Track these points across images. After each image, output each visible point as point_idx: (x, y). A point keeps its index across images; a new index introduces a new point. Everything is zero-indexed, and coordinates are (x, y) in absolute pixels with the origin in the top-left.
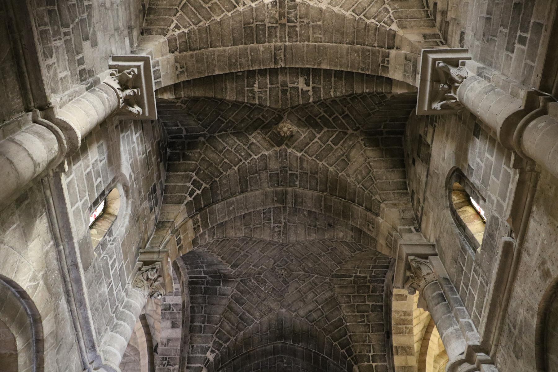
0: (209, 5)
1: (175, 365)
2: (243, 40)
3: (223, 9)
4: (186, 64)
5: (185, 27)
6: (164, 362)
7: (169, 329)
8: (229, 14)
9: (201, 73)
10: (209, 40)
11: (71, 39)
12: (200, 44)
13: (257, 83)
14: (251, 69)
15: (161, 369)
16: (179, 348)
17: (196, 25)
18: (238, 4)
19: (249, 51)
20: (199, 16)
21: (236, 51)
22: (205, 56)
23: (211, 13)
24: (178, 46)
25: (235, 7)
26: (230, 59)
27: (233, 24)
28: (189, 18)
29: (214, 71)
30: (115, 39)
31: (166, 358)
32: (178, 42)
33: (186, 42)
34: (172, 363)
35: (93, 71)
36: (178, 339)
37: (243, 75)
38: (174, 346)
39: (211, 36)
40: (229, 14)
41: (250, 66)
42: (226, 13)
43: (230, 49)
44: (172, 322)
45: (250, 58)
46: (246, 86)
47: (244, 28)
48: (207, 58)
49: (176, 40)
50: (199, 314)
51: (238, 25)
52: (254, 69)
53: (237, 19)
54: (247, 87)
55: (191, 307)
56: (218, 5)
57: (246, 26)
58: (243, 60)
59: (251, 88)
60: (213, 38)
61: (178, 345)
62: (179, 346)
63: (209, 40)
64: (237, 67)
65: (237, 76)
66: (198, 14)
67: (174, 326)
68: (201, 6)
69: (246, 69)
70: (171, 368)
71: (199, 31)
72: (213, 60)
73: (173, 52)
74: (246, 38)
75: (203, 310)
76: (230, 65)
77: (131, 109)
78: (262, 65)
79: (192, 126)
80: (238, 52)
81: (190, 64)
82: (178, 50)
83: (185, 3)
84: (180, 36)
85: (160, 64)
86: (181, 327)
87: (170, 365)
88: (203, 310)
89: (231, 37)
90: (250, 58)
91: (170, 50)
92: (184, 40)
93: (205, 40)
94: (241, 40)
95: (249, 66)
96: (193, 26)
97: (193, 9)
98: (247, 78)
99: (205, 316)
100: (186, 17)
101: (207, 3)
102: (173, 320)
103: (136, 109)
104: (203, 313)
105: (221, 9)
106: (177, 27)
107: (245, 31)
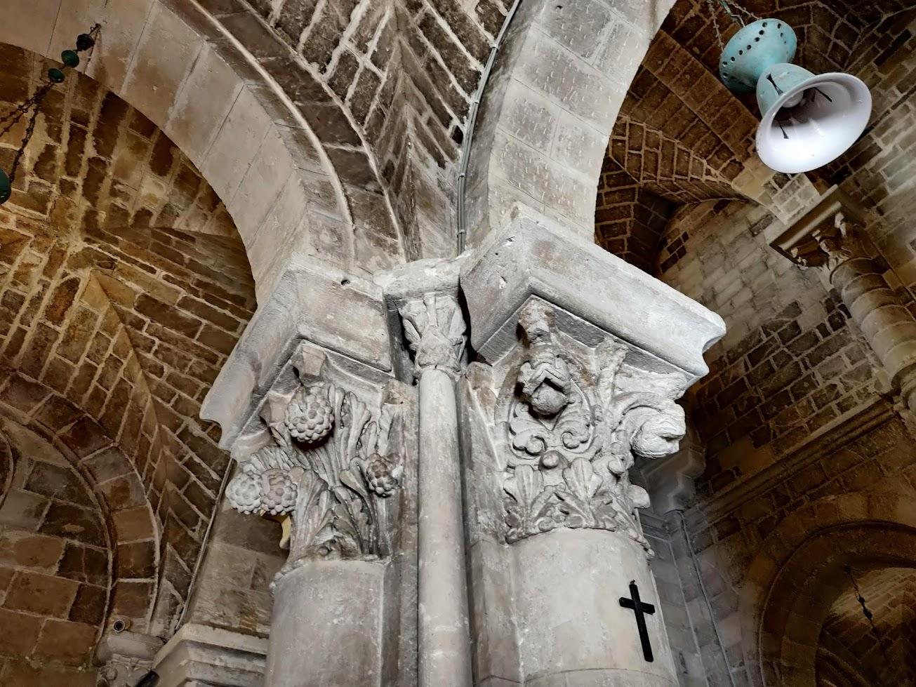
0: (655, 150)
2: (655, 85)
3: (645, 134)
4: (741, 139)
5: (702, 164)
8: (644, 125)
9: (737, 110)
10: (691, 125)
11: (807, 356)
12: (705, 133)
13: (688, 16)
14: (678, 45)
17: (689, 154)
18: (625, 124)
19: (661, 70)
20: (676, 153)
21: (675, 84)
22: (714, 119)
23: (661, 143)
24: (728, 161)
25: (630, 125)
26: (689, 85)
27: (650, 112)
28: (688, 162)
29: (721, 92)
30: (777, 263)
32: (725, 165)
33: (716, 153)
35: (826, 301)
37: (695, 45)
39: (685, 127)
40: (644, 125)
41: (676, 50)
42: (645, 129)
43: (680, 94)
45: (667, 61)
46: (705, 26)
47: (641, 97)
48: (713, 115)
49: (724, 169)
51: (645, 107)
52: (674, 42)
53: (640, 113)
54: (704, 23)
56: (646, 141)
57: (637, 97)
58: (677, 66)
59: (701, 15)
60: (684, 123)
63: (691, 125)
64: (692, 65)
65: (702, 51)
66: (676, 156)
68: (664, 156)
69: (684, 51)
71: (691, 146)
72: (710, 105)
73: (740, 164)
74: (650, 84)
76: (697, 76)
77: (843, 231)
78: (661, 38)
79: (819, 28)
80: (674, 80)
81: (738, 133)
82: (733, 158)
83: (677, 174)
84: (717, 167)
85: (766, 181)
89: (665, 102)
90: (667, 61)
91: (741, 170)
92: (716, 158)
93: (695, 131)
94: (657, 88)
95: (678, 52)
96: (693, 155)
97: (675, 164)
98: (692, 35)
100: (690, 167)
101: (656, 154)
103: (839, 223)
105: (647, 137)
106: (708, 173)
107: (643, 93)
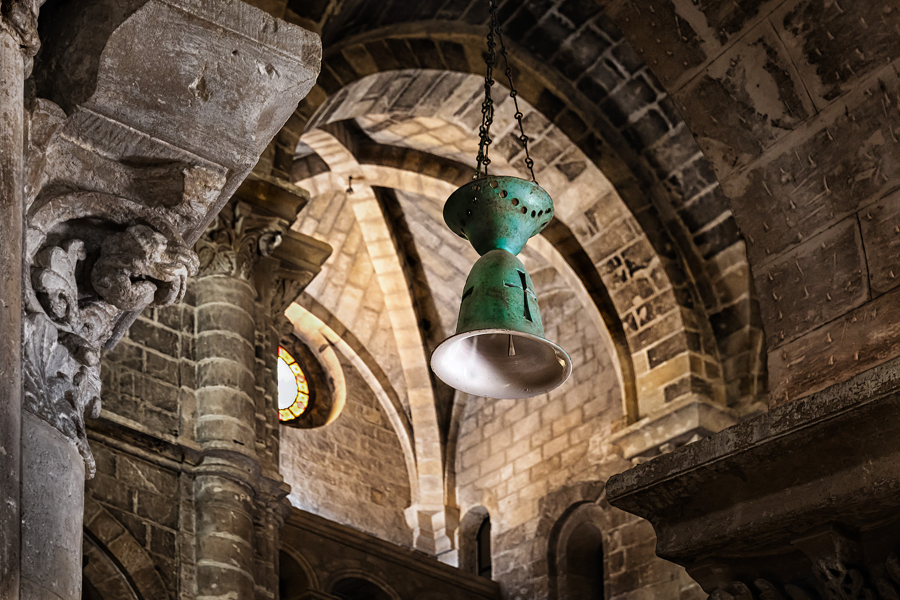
1: (649, 260)
6: (619, 271)
7: (566, 188)
15: (622, 292)
16: (628, 214)
31: (616, 258)
34: (638, 261)
36: (609, 194)
38: (612, 220)
44: (558, 166)
50: (618, 88)
55: (580, 87)
61: (620, 210)
62: (624, 208)
67: (571, 173)
70: (644, 273)
75: (620, 68)
86: (589, 162)
87: (638, 268)
88: (620, 68)
99: (640, 78)
102: (557, 160)
104: (626, 74)
